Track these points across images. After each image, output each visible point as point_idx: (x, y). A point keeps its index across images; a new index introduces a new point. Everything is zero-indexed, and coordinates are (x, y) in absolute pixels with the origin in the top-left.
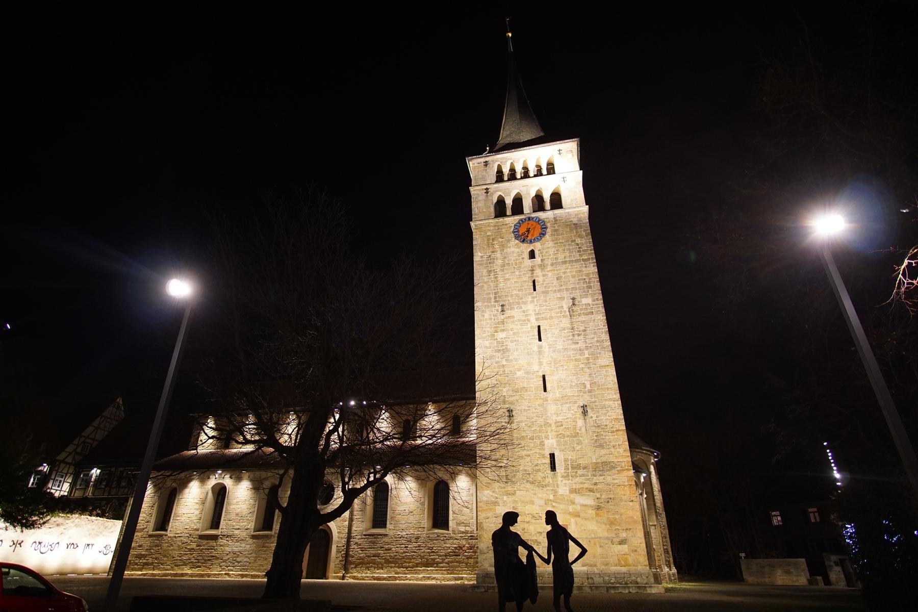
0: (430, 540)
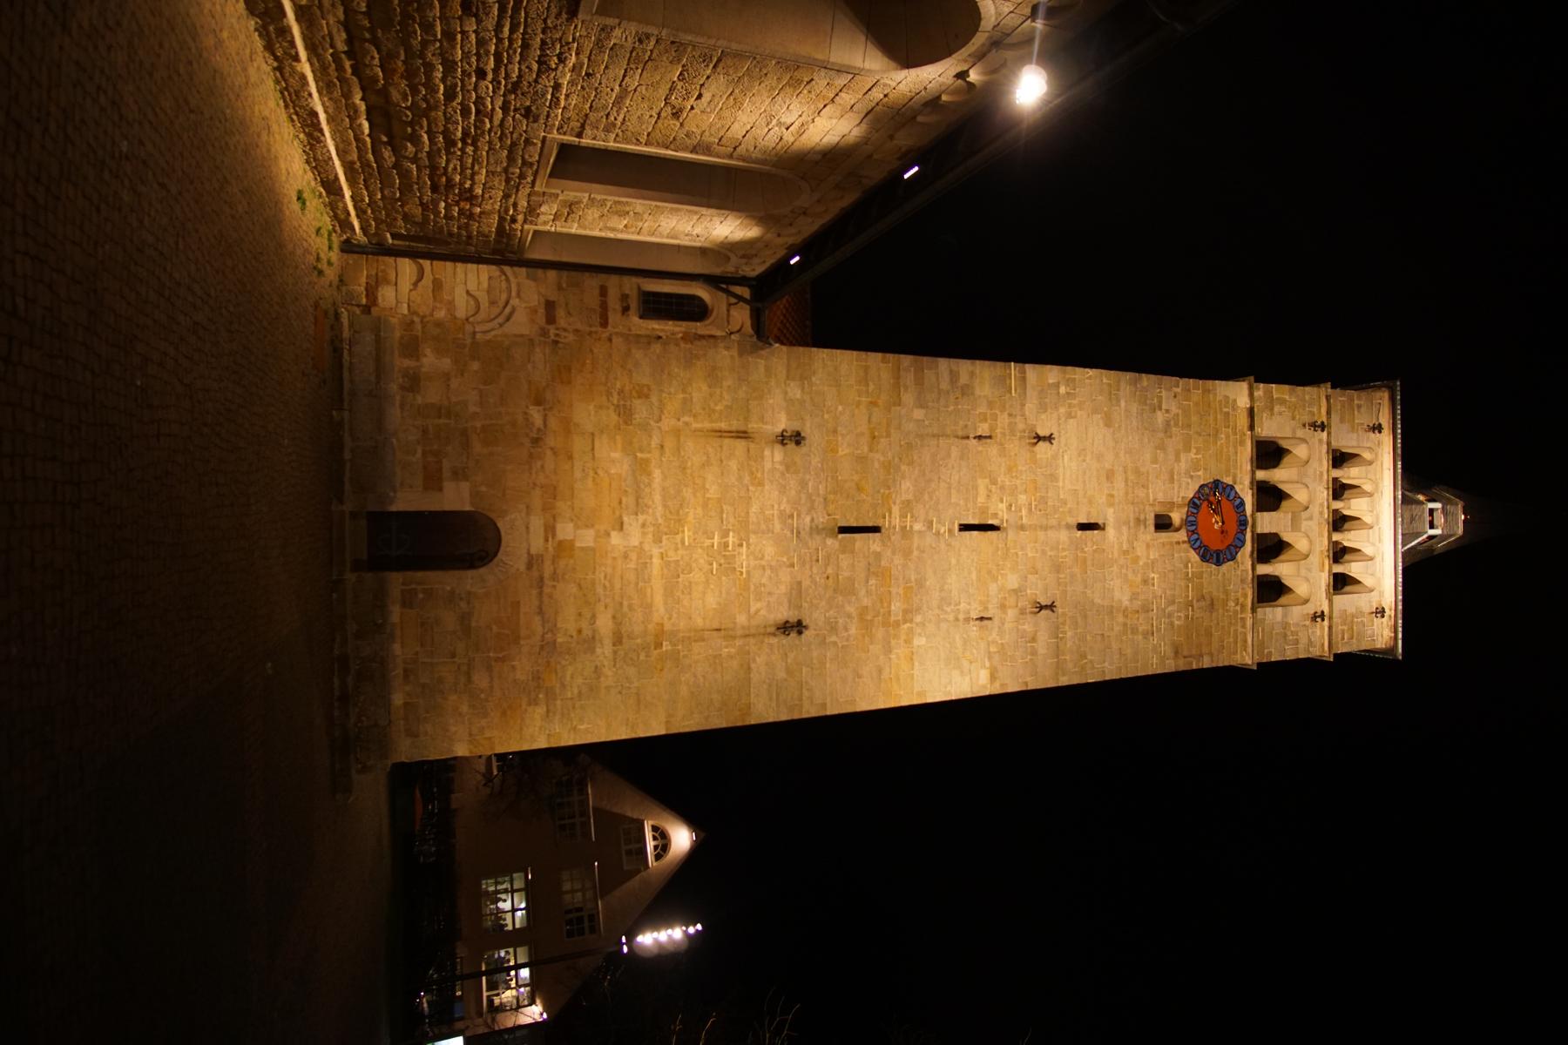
0: (514, 144)
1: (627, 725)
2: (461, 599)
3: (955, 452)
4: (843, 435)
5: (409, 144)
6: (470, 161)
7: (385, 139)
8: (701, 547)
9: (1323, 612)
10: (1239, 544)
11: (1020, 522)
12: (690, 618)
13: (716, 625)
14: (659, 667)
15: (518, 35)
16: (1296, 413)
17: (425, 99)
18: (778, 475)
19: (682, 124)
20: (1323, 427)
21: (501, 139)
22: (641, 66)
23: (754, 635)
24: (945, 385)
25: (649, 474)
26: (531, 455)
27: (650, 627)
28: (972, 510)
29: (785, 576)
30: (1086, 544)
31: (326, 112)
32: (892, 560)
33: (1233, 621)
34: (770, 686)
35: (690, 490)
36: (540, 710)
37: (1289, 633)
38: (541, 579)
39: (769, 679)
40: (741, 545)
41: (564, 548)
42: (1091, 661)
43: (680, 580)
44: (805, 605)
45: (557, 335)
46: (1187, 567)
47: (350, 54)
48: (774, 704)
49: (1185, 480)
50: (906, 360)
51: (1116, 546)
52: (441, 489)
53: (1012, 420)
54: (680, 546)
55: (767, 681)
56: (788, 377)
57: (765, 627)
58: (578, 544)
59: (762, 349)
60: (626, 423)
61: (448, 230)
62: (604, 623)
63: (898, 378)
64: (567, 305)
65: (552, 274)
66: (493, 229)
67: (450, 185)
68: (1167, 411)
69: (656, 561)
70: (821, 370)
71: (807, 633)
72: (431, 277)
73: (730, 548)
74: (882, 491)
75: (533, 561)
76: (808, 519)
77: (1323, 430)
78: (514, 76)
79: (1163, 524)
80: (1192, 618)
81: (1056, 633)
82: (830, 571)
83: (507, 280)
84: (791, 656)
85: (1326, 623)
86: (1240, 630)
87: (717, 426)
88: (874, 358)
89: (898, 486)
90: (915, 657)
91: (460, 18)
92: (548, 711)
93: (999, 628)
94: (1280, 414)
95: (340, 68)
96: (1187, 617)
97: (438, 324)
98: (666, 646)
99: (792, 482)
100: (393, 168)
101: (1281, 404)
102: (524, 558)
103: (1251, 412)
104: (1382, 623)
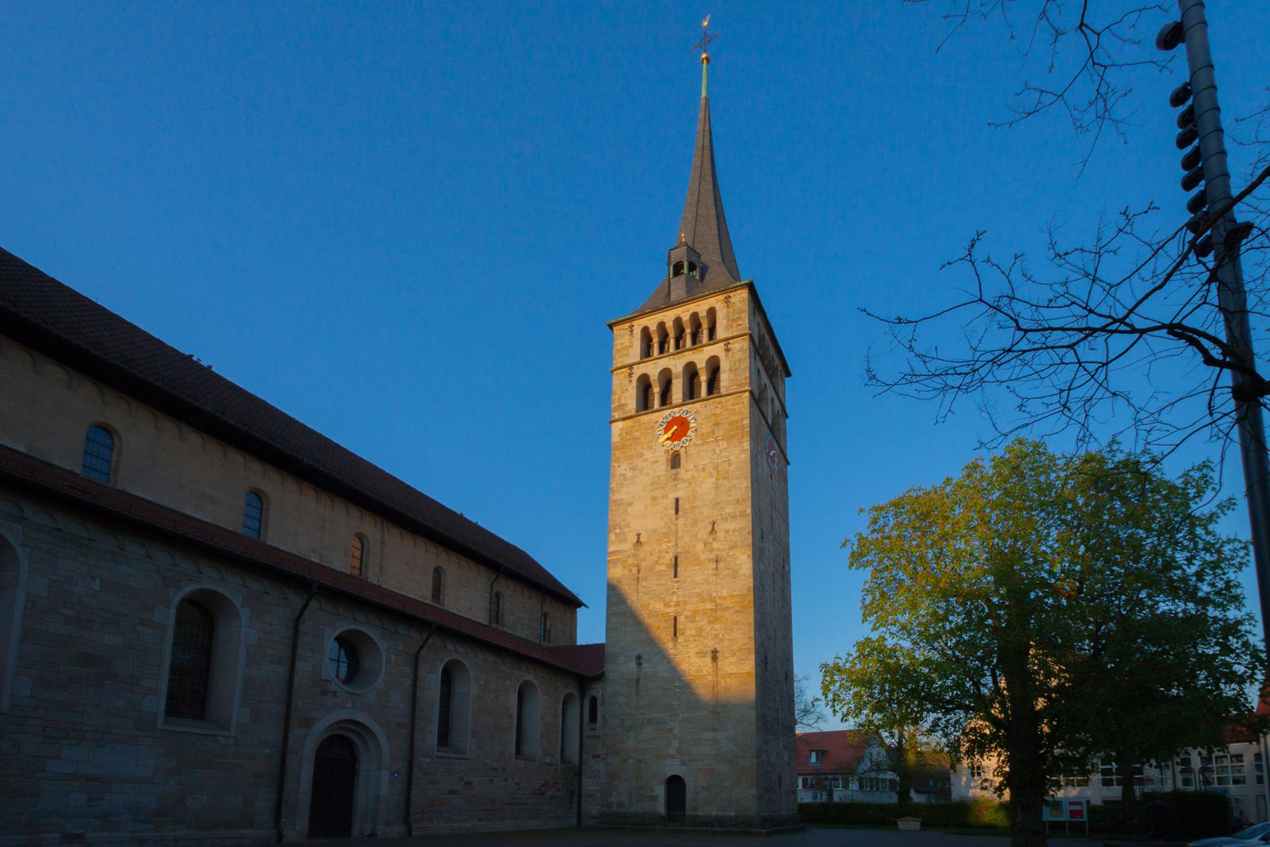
46: (697, 445)
51: (687, 490)
52: (657, 796)
58: (678, 746)
65: (584, 756)
69: (685, 715)
71: (718, 649)
80: (723, 436)
81: (725, 519)
82: (692, 639)
94: (625, 398)
96: (722, 440)
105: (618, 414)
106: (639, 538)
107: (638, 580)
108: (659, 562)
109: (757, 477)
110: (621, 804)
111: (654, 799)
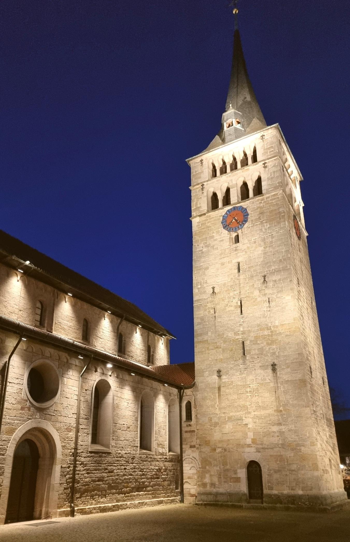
0: (142, 461)
1: (307, 420)
2: (270, 472)
3: (219, 320)
4: (217, 358)
5: (145, 484)
6: (148, 470)
7: (144, 489)
8: (251, 399)
9: (263, 164)
10: (241, 208)
11: (239, 294)
12: (272, 401)
13: (274, 393)
14: (288, 411)
15: (116, 462)
16: (199, 197)
17: (133, 480)
18: (229, 377)
19: (131, 426)
20: (203, 185)
21: (140, 464)
22: (119, 438)
23: (277, 380)
24: (201, 326)
25: (232, 416)
26: (229, 452)
27: (276, 414)
28: (236, 311)
29: (259, 371)
30: (244, 268)
31: (139, 500)
32: (252, 336)
33: (267, 202)
34: (293, 373)
35: (235, 404)
36: (303, 448)
37: (271, 177)
38: (263, 448)
39: (291, 374)
40: (250, 386)
41: (254, 441)
42: (282, 257)
43: (261, 405)
44: (267, 364)
45: (198, 445)
46: (250, 227)
47: (125, 494)
48: (299, 371)
49: (222, 235)
50: (196, 340)
51: (244, 256)
52: (240, 478)
53: (209, 302)
54: (251, 406)
55: (291, 374)
56: (203, 376)
57: (274, 377)
58: (252, 438)
59: (196, 384)
60: (219, 424)
61: (172, 475)
62: (275, 429)
63: (200, 342)
64: (190, 442)
65: (184, 446)
66: (170, 463)
67: (156, 475)
68: (203, 247)
69: (256, 413)
70: (201, 366)
72: (187, 479)
73: (251, 390)
74: (232, 343)
75: (258, 451)
76: (241, 366)
77: (204, 185)
78: (124, 462)
79: (237, 240)
80: (267, 220)
81: (273, 273)
82: (256, 357)
83: (186, 459)
84: (283, 367)
85: (267, 161)
86: (270, 199)
87: (217, 397)
88: (196, 350)
89: (230, 337)
90: (282, 324)
91: (114, 473)
92: (303, 446)
93: (272, 295)
95: (128, 496)
97: (198, 477)
98: (281, 408)
99: (231, 372)
100: (153, 488)
101: (197, 204)
102: (257, 453)
103: (200, 216)
104: (266, 135)
105: (196, 213)
106: (214, 290)
107: (215, 318)
108: (229, 305)
109: (291, 244)
110: (213, 485)
111: (238, 480)
